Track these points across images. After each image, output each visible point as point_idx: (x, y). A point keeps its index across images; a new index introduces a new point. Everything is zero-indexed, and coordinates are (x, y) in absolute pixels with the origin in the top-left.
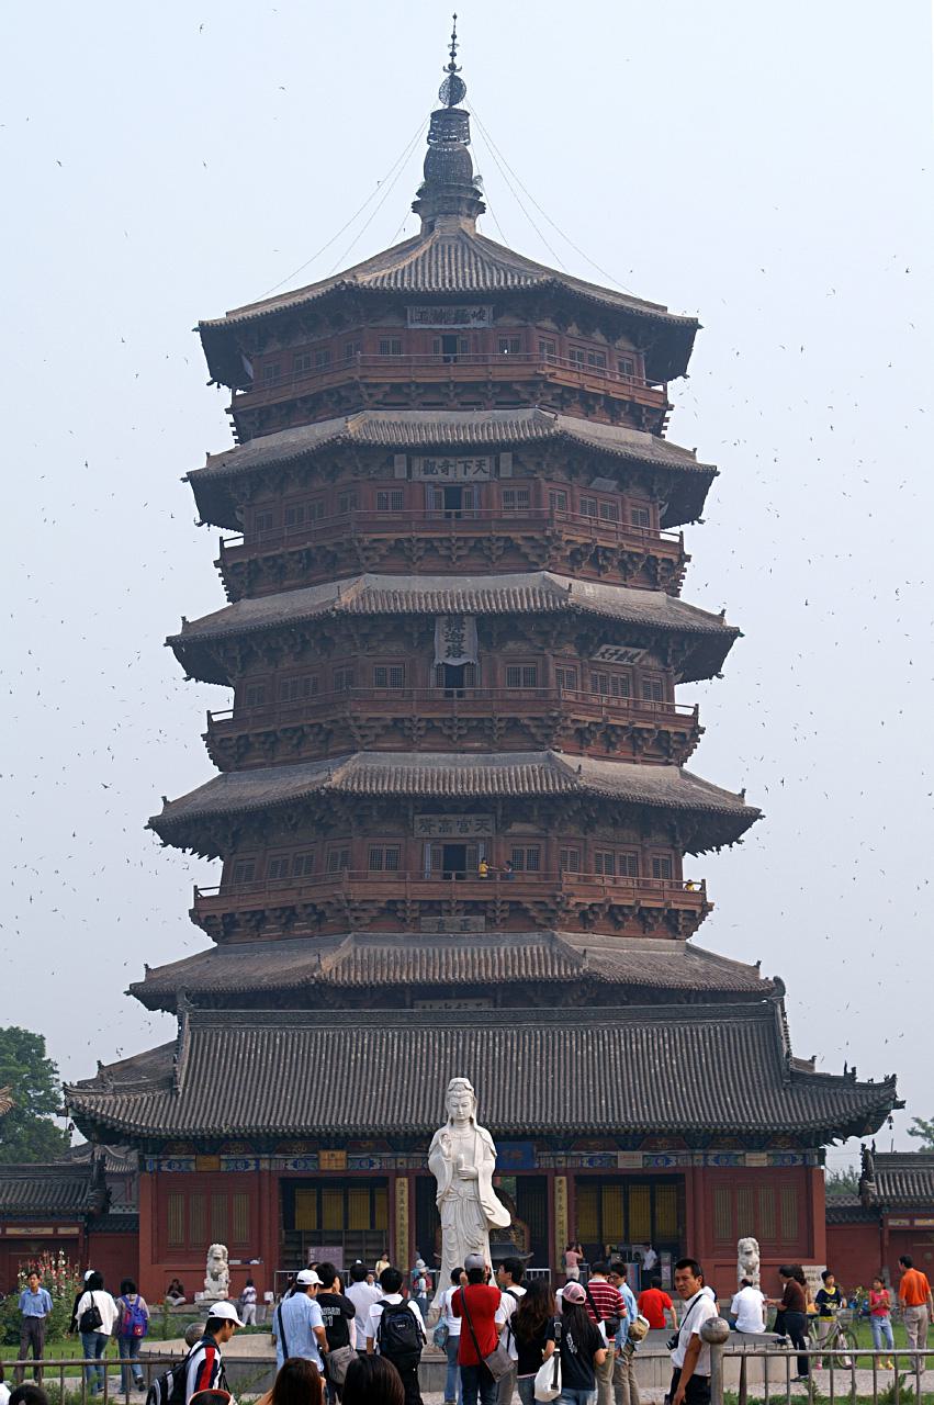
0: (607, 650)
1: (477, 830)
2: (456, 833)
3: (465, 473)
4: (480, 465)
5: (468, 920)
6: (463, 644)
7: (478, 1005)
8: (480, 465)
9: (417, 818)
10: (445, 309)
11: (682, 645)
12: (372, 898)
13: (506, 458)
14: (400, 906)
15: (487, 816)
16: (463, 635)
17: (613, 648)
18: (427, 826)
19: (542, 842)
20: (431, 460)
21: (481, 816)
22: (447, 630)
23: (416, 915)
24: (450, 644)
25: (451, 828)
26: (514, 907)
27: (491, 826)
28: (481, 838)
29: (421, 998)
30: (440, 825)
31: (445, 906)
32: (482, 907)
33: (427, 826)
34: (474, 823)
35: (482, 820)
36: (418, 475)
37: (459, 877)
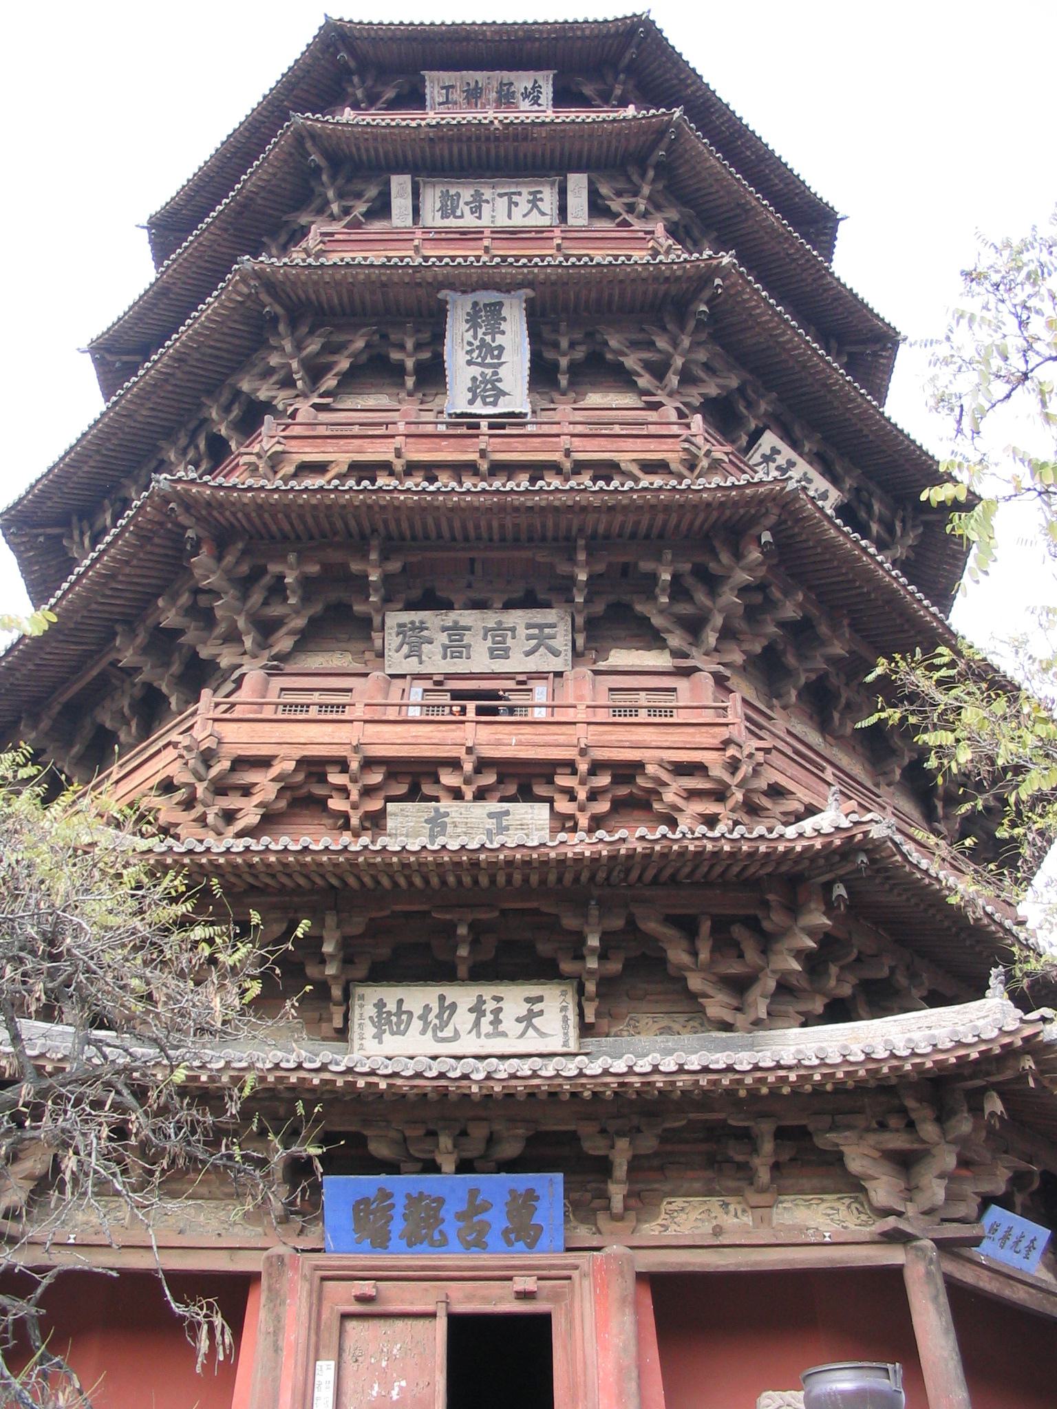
0: (775, 451)
1: (528, 654)
2: (480, 660)
3: (510, 217)
4: (534, 202)
5: (507, 813)
6: (502, 371)
7: (528, 1000)
8: (534, 202)
9: (395, 618)
10: (480, 76)
11: (890, 529)
12: (264, 751)
13: (578, 183)
14: (335, 778)
15: (550, 616)
16: (501, 348)
17: (787, 453)
18: (415, 639)
19: (681, 684)
20: (452, 192)
21: (538, 616)
22: (469, 336)
23: (375, 805)
24: (476, 371)
25: (468, 647)
26: (623, 791)
27: (562, 641)
28: (540, 676)
29: (382, 974)
30: (443, 638)
31: (449, 779)
32: (539, 790)
33: (415, 639)
34: (522, 632)
35: (541, 627)
36: (432, 217)
37: (480, 711)
